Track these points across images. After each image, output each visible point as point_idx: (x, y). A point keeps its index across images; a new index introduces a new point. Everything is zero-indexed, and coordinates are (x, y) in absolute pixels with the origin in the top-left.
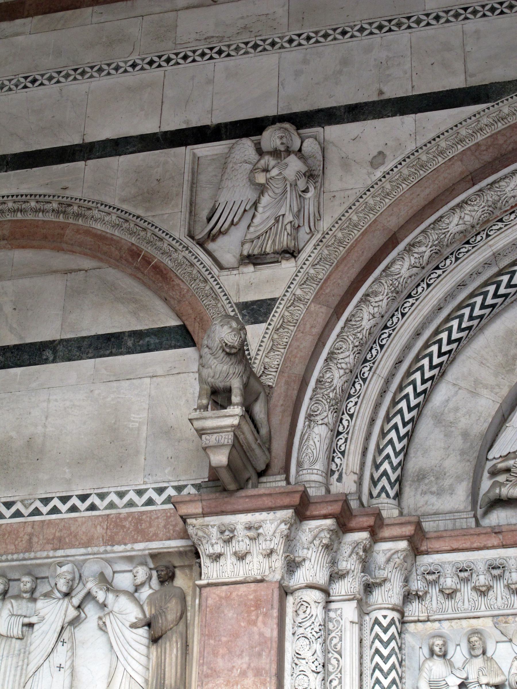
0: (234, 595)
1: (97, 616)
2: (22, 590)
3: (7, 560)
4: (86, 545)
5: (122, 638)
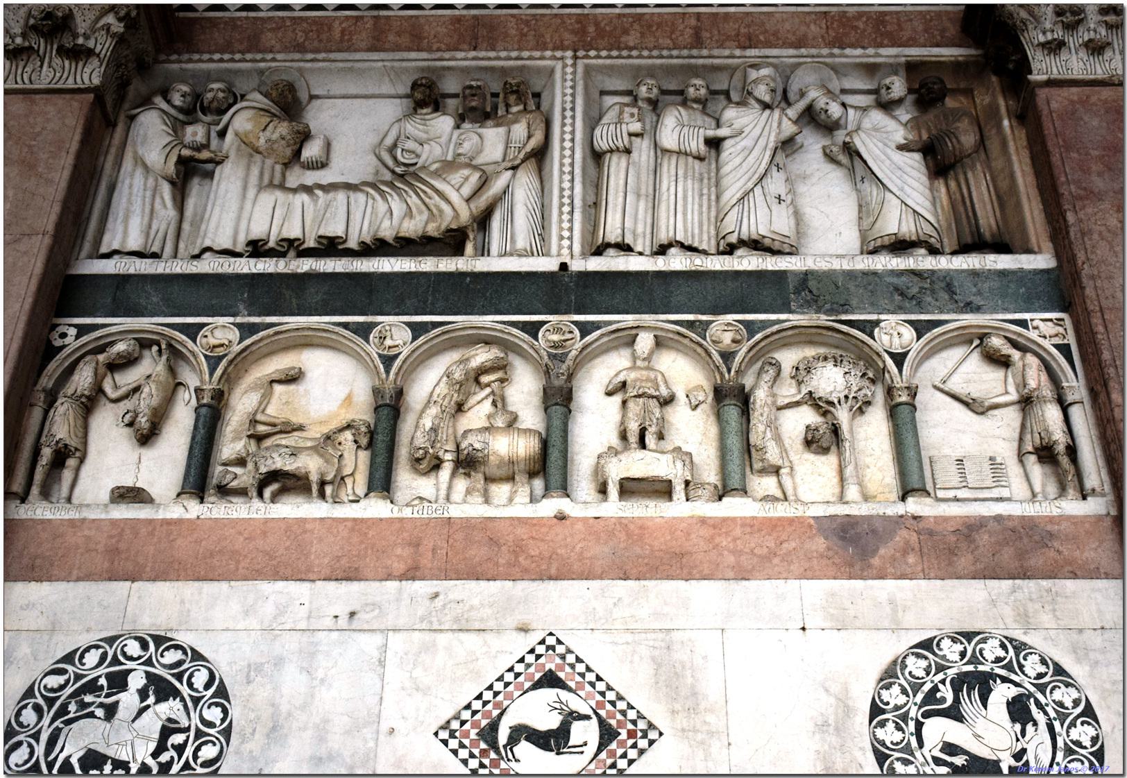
0: (1094, 99)
1: (820, 146)
2: (693, 96)
3: (662, 57)
4: (797, 46)
5: (888, 162)
